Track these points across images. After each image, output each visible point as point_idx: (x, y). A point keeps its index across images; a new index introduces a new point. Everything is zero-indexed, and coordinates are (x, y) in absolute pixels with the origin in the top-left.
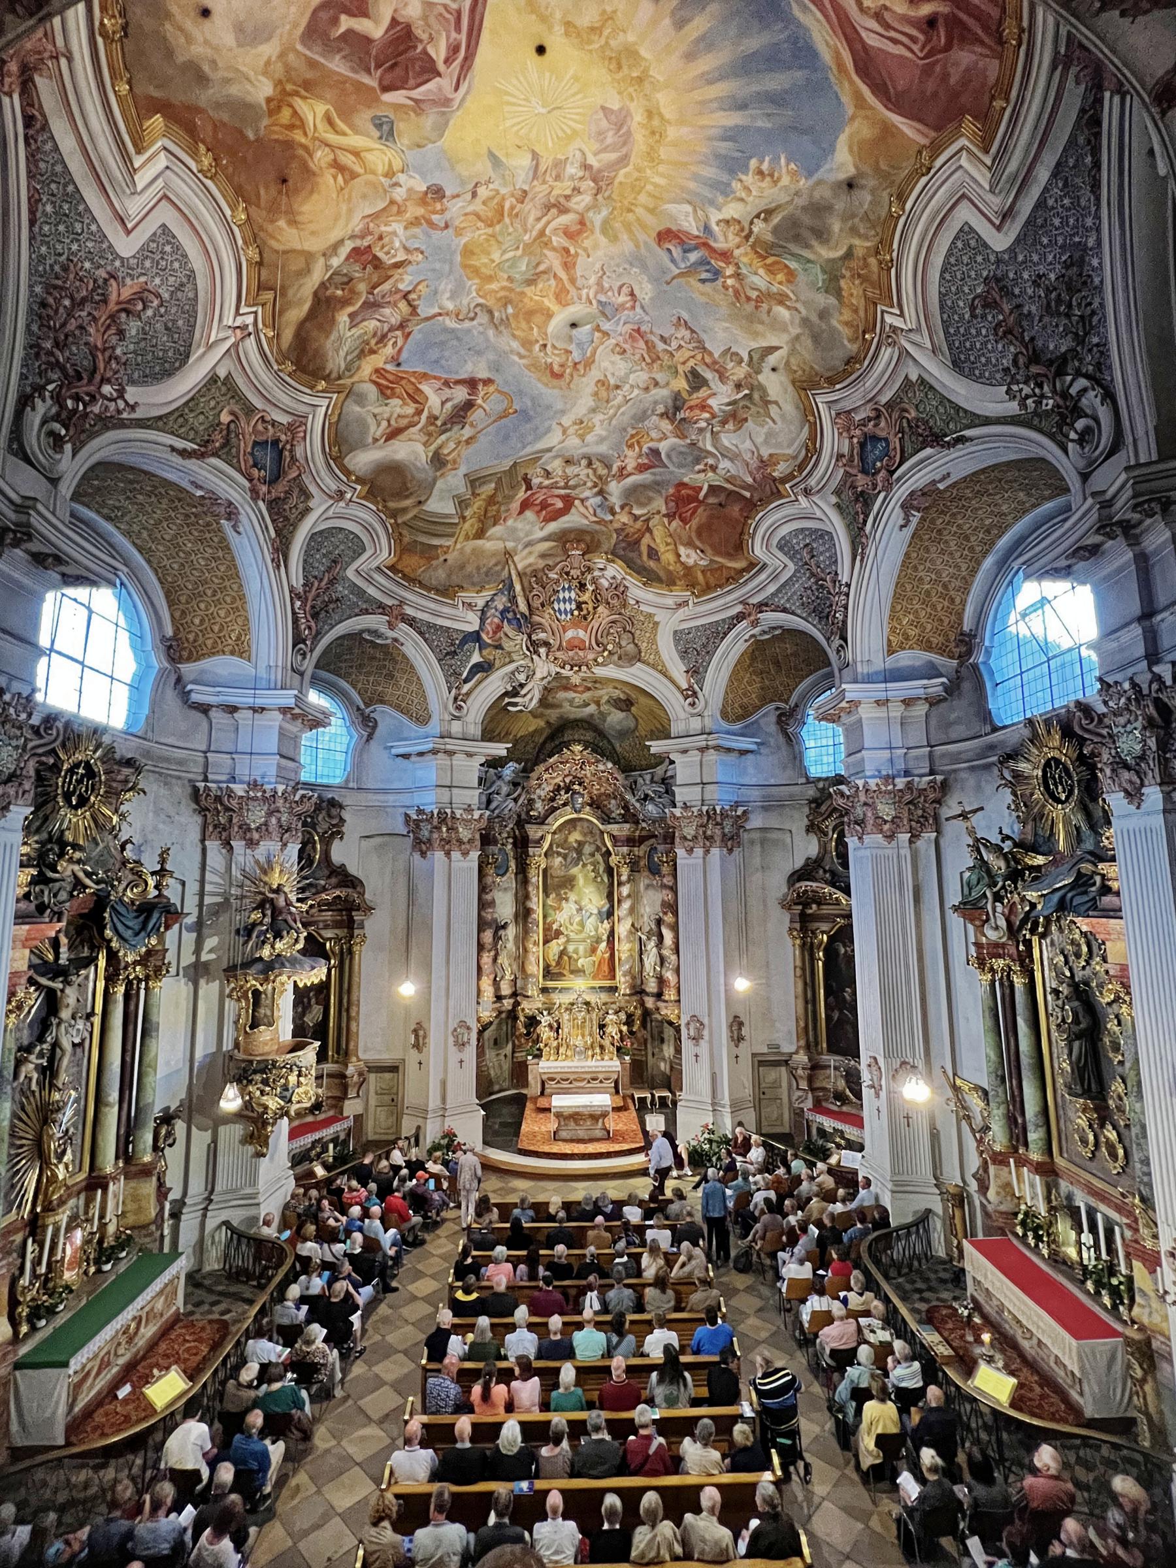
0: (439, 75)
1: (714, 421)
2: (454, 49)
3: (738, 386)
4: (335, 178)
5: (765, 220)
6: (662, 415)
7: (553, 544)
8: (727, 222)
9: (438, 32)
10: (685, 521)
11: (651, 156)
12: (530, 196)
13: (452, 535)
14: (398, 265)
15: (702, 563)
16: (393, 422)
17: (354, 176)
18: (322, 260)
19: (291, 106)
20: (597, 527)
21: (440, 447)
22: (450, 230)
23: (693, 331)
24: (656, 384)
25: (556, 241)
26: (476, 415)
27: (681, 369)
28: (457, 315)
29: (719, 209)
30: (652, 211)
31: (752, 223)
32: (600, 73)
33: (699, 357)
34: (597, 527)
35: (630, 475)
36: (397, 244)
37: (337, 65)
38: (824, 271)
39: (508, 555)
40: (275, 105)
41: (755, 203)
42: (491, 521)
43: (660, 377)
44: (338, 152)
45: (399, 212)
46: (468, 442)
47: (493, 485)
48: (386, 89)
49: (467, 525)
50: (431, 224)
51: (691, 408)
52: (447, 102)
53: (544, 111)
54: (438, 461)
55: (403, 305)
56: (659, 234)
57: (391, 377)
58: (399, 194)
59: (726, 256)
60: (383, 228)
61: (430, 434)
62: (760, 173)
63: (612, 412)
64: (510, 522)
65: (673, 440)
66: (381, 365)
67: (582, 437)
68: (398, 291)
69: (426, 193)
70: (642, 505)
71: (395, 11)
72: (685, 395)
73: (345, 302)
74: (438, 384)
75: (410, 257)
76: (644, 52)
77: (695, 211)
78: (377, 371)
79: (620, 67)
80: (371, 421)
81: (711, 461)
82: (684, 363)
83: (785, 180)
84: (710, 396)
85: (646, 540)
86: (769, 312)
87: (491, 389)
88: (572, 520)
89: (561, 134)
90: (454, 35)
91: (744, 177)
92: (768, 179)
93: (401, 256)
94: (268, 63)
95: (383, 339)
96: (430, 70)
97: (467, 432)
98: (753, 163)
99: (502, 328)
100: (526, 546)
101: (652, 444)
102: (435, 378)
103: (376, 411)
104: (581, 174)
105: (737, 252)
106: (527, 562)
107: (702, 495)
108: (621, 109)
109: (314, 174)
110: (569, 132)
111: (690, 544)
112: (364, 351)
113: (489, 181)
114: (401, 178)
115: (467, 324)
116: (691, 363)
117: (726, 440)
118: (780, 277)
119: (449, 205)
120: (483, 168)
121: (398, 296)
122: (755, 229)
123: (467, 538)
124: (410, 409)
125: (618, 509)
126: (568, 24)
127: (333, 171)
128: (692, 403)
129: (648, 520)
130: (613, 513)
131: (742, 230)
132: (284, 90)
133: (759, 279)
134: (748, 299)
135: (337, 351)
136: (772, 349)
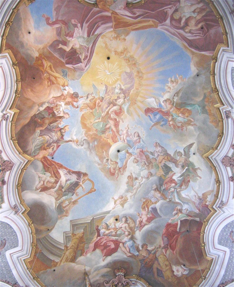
0: (82, 63)
1: (177, 187)
2: (86, 57)
3: (183, 167)
4: (48, 83)
5: (177, 96)
6: (155, 190)
7: (108, 269)
8: (166, 101)
9: (83, 52)
10: (173, 249)
11: (140, 85)
12: (104, 99)
13: (60, 257)
14: (60, 117)
15: (186, 273)
16: (45, 183)
17: (53, 83)
18: (37, 106)
19: (42, 61)
20: (131, 259)
21: (62, 203)
22: (79, 109)
23: (162, 147)
24: (151, 175)
25: (113, 116)
26: (79, 190)
27: (160, 166)
28: (77, 143)
29: (163, 97)
30: (142, 102)
31: (173, 98)
32: (124, 63)
33: (166, 158)
34: (131, 259)
35: (144, 226)
36: (61, 110)
37: (56, 55)
38: (199, 106)
39: (86, 274)
40: (38, 59)
41: (173, 92)
42: (79, 253)
43: (153, 171)
44: (51, 76)
45: (64, 99)
46: (75, 202)
47: (82, 230)
48: (68, 63)
49: (67, 253)
50: (73, 105)
51: (166, 183)
52: (83, 70)
53: (109, 74)
54: (61, 209)
55: (59, 133)
56: (145, 110)
57: (49, 163)
58: (65, 93)
59: (167, 113)
60: (58, 103)
61: (59, 195)
62: (172, 82)
63: (135, 191)
64: (88, 255)
65: (161, 202)
66: (46, 156)
67: (122, 205)
68: (58, 127)
69: (73, 94)
70: (152, 243)
71: (73, 46)
72: (163, 178)
73: (41, 125)
74: (66, 171)
75: (64, 116)
76: (135, 57)
77: (156, 100)
78: (45, 158)
79: (129, 61)
80: (37, 179)
81: (179, 207)
82: (161, 163)
83: (180, 81)
84: (173, 175)
85: (155, 266)
86: (186, 130)
87: (86, 178)
88: (118, 255)
89: (114, 80)
90: (86, 53)
91: (167, 85)
92: (175, 83)
93: (61, 115)
94: (40, 49)
95: (49, 145)
96: (79, 61)
97: (74, 198)
98: (169, 79)
99: (92, 151)
100: (95, 271)
101: (152, 206)
102: (65, 168)
103: (41, 175)
104: (120, 92)
105: (171, 110)
106: (95, 279)
107: (178, 230)
108: (130, 72)
109: (42, 79)
110: (116, 79)
111: (178, 263)
112: (43, 147)
113: (92, 94)
114: (67, 88)
115: (80, 147)
116: (163, 162)
117: (184, 194)
118: (186, 114)
119: (79, 100)
120: (92, 90)
121: (59, 129)
122: (175, 100)
123: (67, 260)
124: (53, 180)
125: (141, 248)
126: (116, 52)
127: (48, 80)
128: (167, 180)
129: (155, 253)
130: (138, 250)
131: (171, 102)
132: (41, 56)
133: (180, 118)
134: (179, 127)
135: (33, 144)
136: (191, 145)
